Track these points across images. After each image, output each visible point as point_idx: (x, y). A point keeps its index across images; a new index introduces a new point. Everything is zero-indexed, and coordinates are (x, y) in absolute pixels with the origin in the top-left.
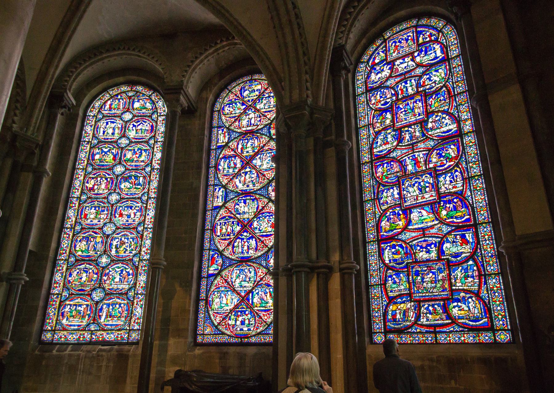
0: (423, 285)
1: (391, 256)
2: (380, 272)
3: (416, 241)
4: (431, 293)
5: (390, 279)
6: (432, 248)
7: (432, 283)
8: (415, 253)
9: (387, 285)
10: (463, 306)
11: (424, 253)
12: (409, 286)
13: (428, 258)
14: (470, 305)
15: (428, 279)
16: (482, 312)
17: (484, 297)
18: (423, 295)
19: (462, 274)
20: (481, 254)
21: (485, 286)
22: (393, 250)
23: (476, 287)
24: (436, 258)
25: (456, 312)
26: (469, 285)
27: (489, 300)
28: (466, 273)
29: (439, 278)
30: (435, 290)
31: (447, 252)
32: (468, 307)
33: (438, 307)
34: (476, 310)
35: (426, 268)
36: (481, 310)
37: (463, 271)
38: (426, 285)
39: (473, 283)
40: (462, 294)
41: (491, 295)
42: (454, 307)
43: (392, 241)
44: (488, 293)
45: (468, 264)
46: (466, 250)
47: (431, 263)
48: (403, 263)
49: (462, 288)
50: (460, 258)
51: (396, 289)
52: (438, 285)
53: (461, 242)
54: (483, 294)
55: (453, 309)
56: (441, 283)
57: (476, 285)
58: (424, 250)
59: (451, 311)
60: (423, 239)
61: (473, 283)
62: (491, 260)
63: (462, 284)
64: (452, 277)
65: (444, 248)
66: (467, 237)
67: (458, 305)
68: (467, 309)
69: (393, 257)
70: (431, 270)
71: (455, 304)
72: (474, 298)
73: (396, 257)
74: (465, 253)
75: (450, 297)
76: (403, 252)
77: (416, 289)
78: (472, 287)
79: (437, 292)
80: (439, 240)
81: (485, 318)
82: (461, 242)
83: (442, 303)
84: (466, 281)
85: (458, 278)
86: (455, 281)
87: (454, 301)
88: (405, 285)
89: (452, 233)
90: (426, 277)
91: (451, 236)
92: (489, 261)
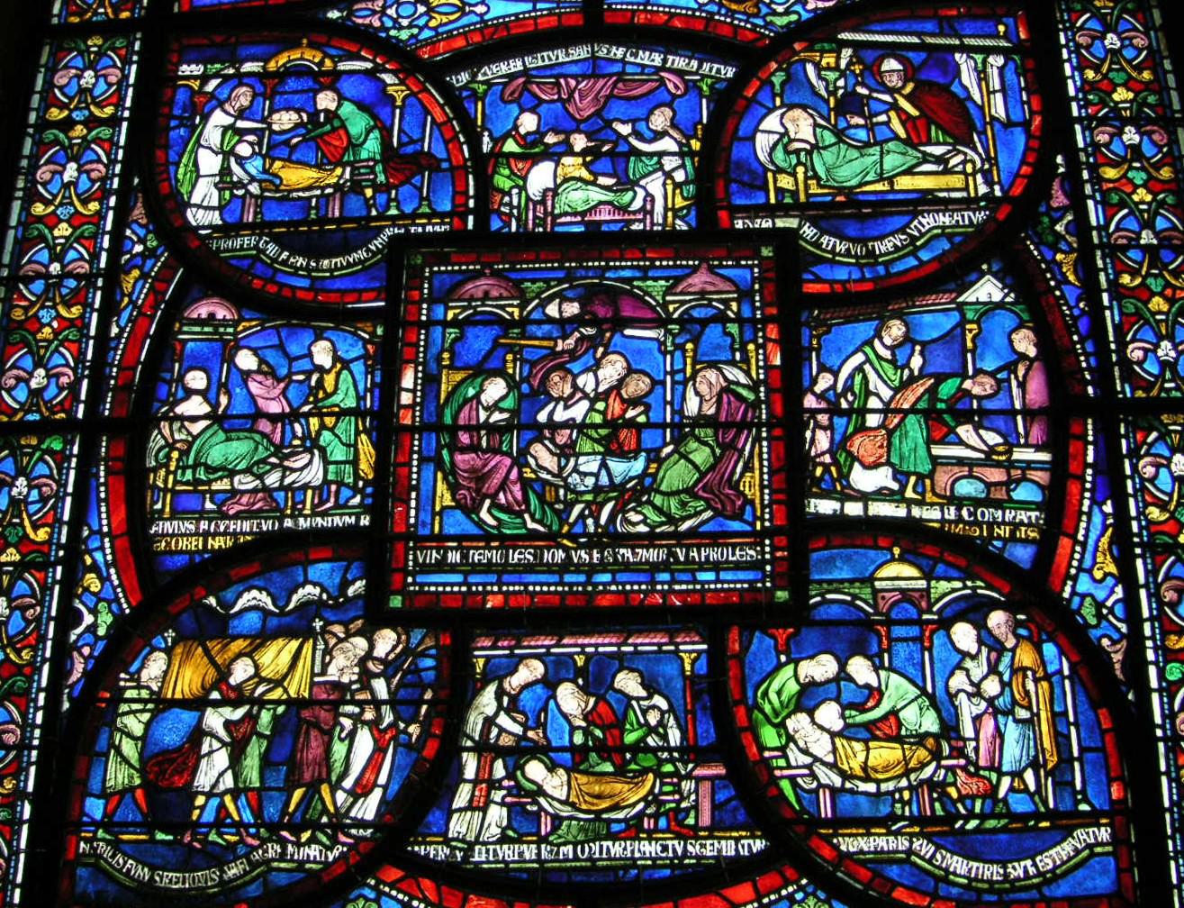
0: (520, 460)
1: (255, 166)
2: (109, 311)
3: (516, 65)
4: (594, 542)
5: (197, 380)
6: (658, 135)
7: (612, 448)
8: (484, 166)
9: (156, 441)
10: (898, 690)
11: (572, 165)
12: (381, 465)
13: (604, 215)
14: (958, 681)
15: (578, 411)
16: (1066, 761)
17: (1088, 612)
18: (514, 557)
19: (904, 385)
20: (1081, 226)
21: (1108, 508)
22: (285, 120)
23: (1022, 516)
24: (681, 226)
25: (821, 747)
26: (966, 488)
27: (1135, 640)
28: (940, 378)
29: (692, 406)
30: (637, 521)
31: (785, 182)
32: (942, 704)
33: (651, 687)
34: (1012, 732)
35: (572, 309)
36: (1061, 739)
37: (916, 362)
38: (549, 461)
39: (996, 475)
40: (898, 573)
41: (1155, 595)
42: (808, 697)
43: (296, 45)
44: (1126, 576)
45: (969, 296)
46: (957, 181)
47: (622, 270)
48: (366, 228)
49: (901, 512)
50: (898, 240)
51: (246, 482)
52: (676, 475)
53: (914, 112)
54: (1084, 584)
55: (799, 722)
56: (702, 456)
57: (1021, 493)
58: (579, 142)
59: (770, 737)
60: (581, 52)
61: (996, 475)
62: (1155, 285)
63: (900, 475)
64: (810, 402)
65: (763, 142)
66: (968, 77)
67: (843, 675)
68: (930, 723)
69: (270, 180)
70: (619, 324)
71: (822, 667)
72: (997, 619)
73: (296, 176)
74: (946, 205)
75: (782, 595)
76: (372, 146)
77: (444, 497)
78: (989, 514)
79: (650, 539)
80: (730, 72)
81: (1092, 819)
82: (914, 112)
83: (691, 650)
84: (937, 450)
85: (873, 420)
86: (840, 445)
87: (811, 636)
88: (339, 453)
89: (844, 36)
90: (559, 386)
91: (829, 60)
92: (1144, 293)
